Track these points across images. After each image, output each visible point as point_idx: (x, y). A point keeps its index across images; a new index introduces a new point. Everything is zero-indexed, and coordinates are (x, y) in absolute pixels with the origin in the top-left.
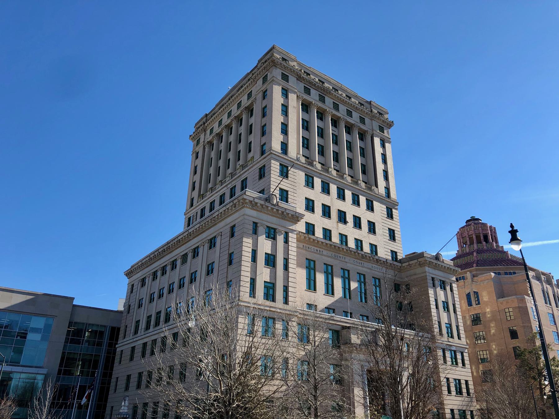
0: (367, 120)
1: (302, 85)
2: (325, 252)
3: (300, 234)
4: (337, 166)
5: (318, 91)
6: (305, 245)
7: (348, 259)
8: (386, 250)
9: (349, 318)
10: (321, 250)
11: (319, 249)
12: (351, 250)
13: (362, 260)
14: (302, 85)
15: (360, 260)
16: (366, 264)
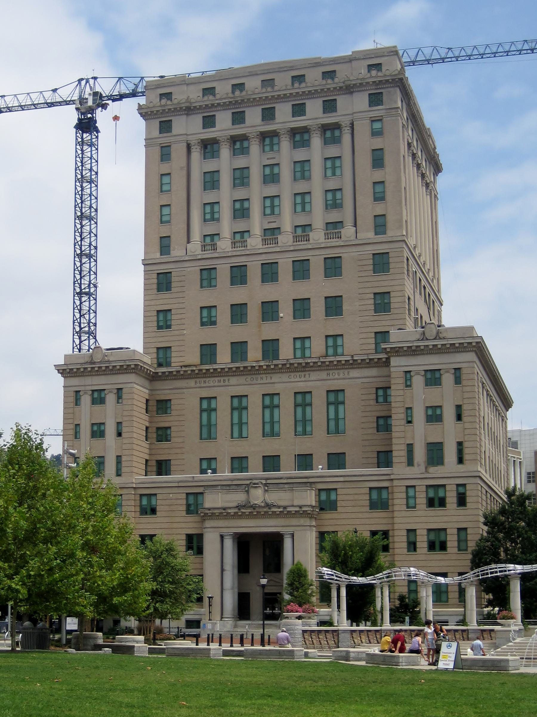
0: (342, 101)
1: (197, 120)
2: (233, 380)
3: (184, 369)
4: (275, 222)
5: (229, 109)
6: (198, 380)
7: (276, 378)
8: (364, 336)
9: (227, 474)
10: (226, 378)
11: (222, 379)
12: (276, 363)
13: (303, 371)
14: (197, 120)
15: (302, 371)
16: (314, 376)
